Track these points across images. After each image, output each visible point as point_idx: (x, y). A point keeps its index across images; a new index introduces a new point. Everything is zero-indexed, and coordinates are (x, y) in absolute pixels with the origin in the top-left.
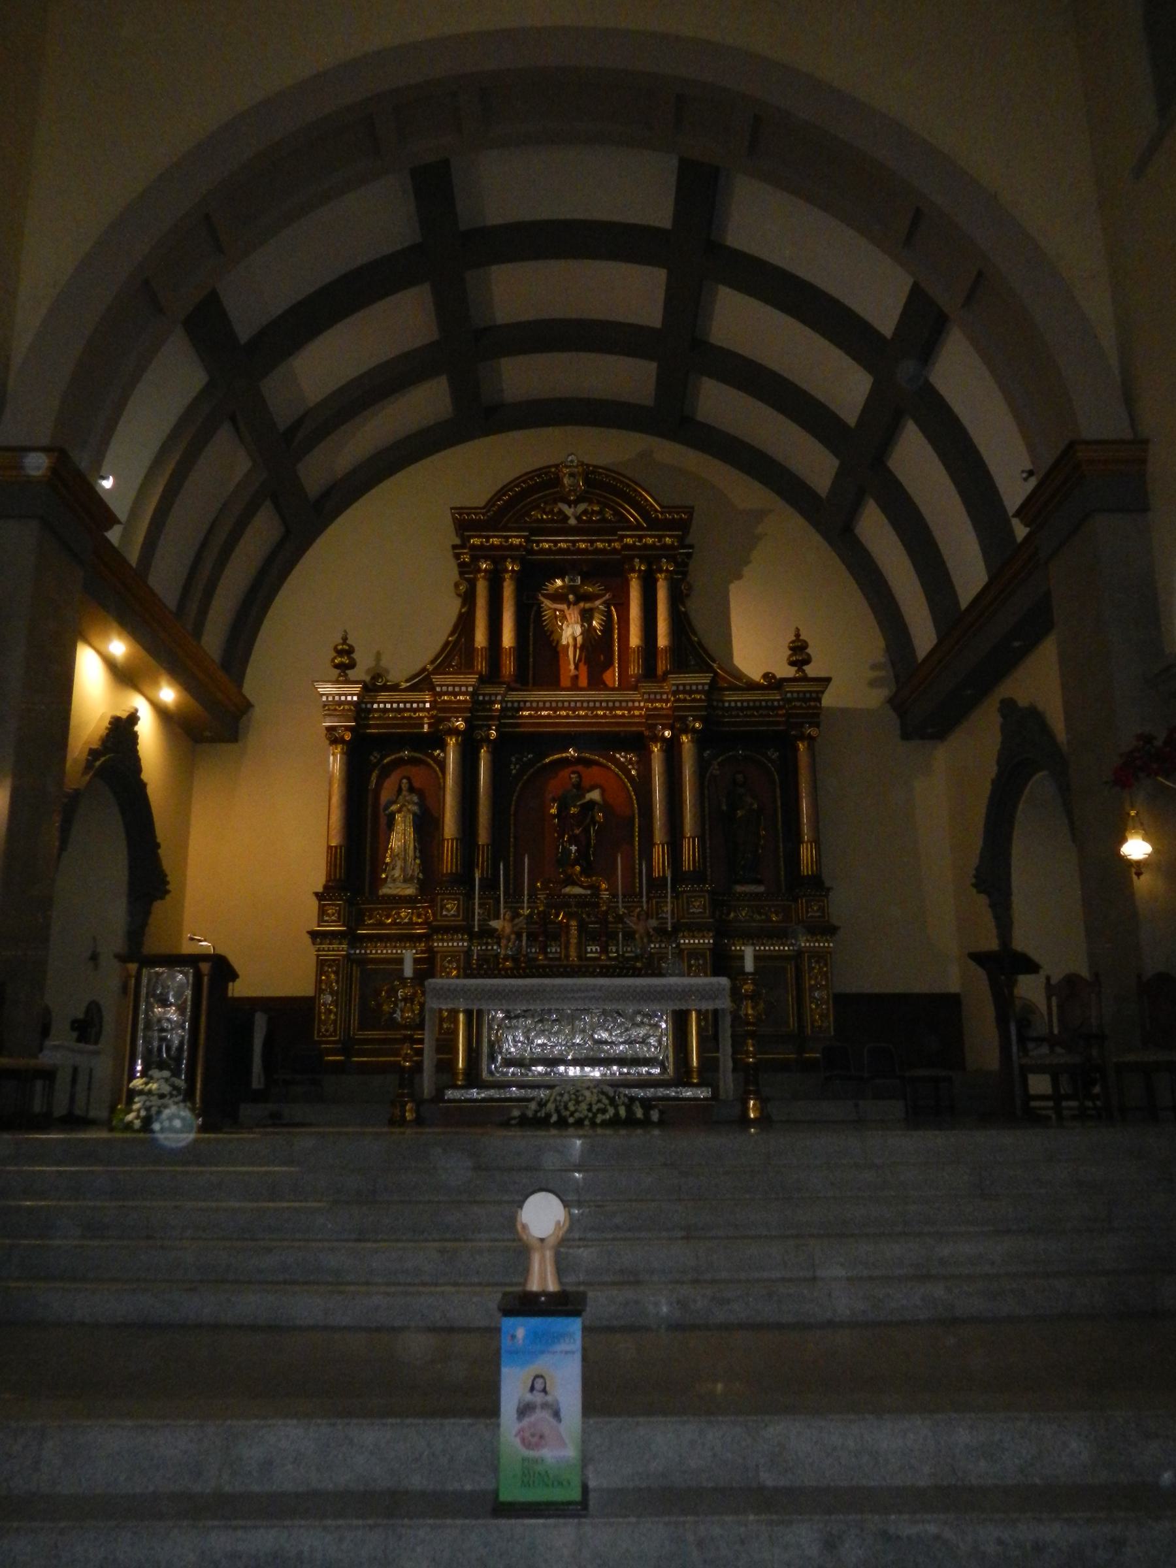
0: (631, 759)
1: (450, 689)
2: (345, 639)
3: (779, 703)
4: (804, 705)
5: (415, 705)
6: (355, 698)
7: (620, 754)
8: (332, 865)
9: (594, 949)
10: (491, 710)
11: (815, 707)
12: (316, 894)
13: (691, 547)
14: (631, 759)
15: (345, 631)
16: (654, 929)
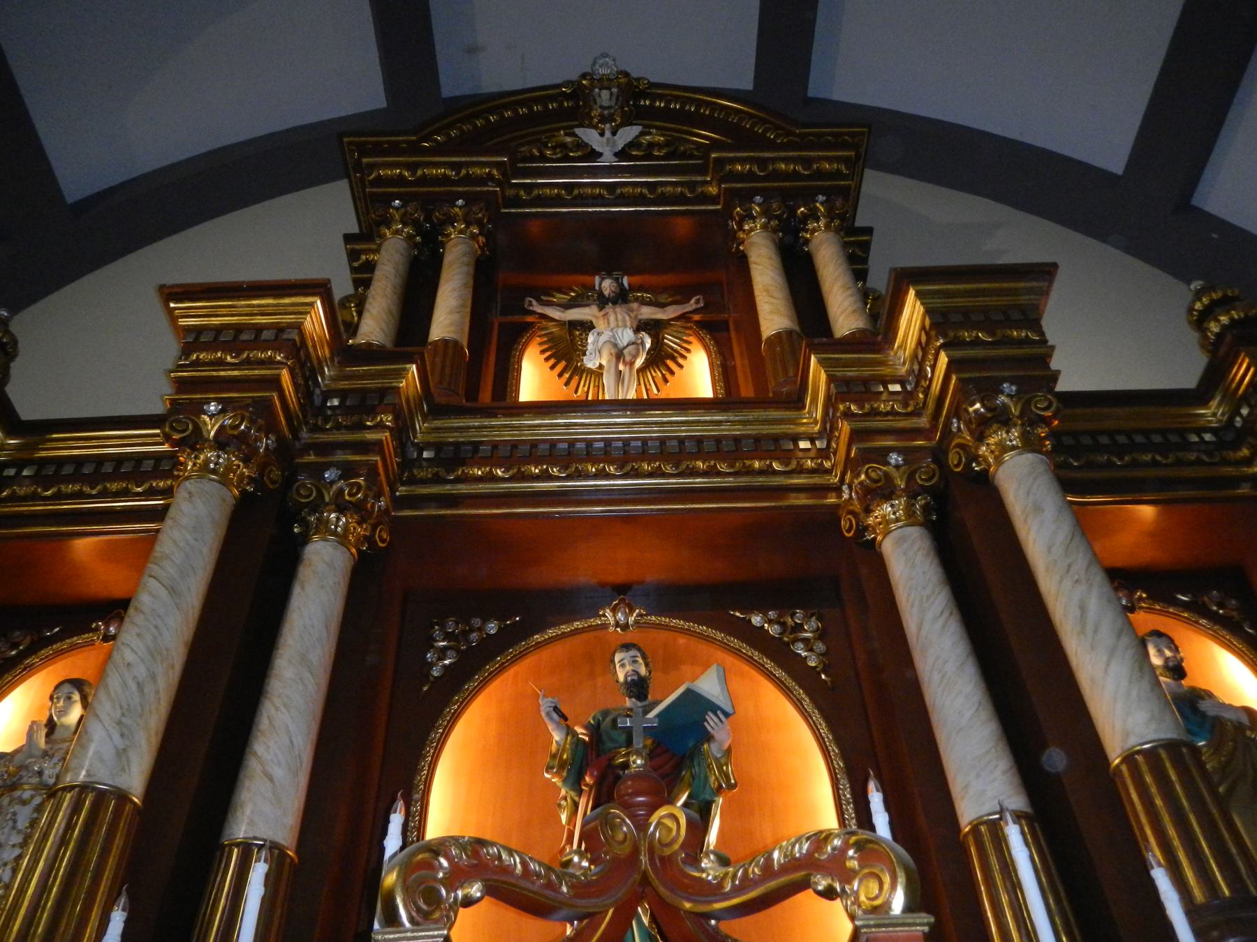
13: (869, 231)
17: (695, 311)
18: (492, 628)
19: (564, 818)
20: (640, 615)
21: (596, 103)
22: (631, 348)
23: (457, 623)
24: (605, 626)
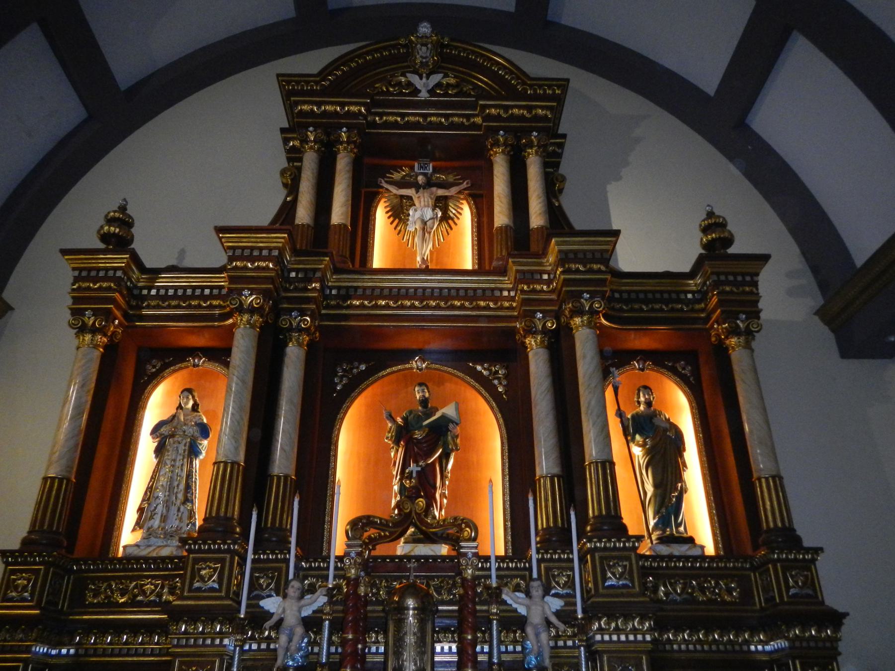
0: (497, 372)
1: (247, 253)
2: (123, 209)
3: (693, 295)
4: (735, 290)
6: (119, 273)
7: (482, 365)
8: (42, 506)
9: (446, 648)
10: (306, 290)
11: (751, 293)
13: (564, 136)
14: (497, 372)
16: (558, 614)
17: (465, 189)
18: (363, 367)
19: (392, 454)
20: (428, 364)
21: (418, 53)
22: (431, 221)
23: (347, 364)
24: (412, 368)
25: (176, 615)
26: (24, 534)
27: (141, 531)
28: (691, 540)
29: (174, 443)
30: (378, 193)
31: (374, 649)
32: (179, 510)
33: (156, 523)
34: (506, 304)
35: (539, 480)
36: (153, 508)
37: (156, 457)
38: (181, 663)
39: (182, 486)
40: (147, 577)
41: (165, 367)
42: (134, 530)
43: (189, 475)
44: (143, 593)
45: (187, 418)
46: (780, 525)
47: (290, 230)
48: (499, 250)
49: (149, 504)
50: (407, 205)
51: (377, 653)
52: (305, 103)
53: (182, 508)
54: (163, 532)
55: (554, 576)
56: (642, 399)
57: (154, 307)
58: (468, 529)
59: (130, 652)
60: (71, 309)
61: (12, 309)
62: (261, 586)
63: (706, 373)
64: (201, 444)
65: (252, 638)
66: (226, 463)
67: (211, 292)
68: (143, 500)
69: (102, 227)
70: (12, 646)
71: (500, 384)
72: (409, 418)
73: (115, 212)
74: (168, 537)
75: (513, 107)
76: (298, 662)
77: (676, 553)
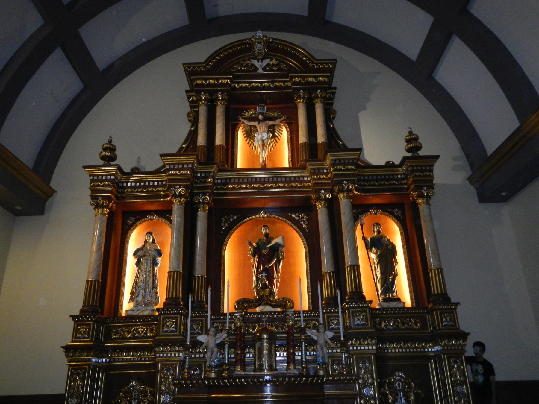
1: (176, 166)
2: (110, 142)
3: (401, 176)
4: (421, 174)
5: (156, 183)
6: (113, 177)
7: (295, 214)
8: (88, 294)
9: (282, 354)
10: (206, 182)
11: (430, 175)
12: (73, 317)
13: (335, 88)
14: (302, 218)
15: (111, 137)
17: (283, 120)
18: (235, 217)
19: (252, 261)
21: (256, 48)
22: (266, 140)
24: (260, 217)
25: (158, 344)
26: (81, 307)
27: (133, 303)
28: (399, 300)
29: (145, 260)
30: (238, 124)
31: (248, 355)
32: (150, 292)
33: (140, 299)
34: (306, 184)
35: (324, 274)
36: (138, 292)
37: (137, 266)
38: (162, 365)
39: (151, 281)
40: (139, 325)
41: (136, 221)
42: (129, 302)
43: (154, 275)
44: (138, 333)
45: (150, 247)
46: (440, 292)
47: (197, 154)
48: (302, 156)
49: (136, 290)
50: (253, 130)
51: (249, 357)
52: (198, 79)
53: (152, 291)
54: (144, 303)
55: (331, 320)
56: (375, 230)
57: (130, 192)
58: (289, 303)
59: (135, 360)
60: (90, 196)
61: (55, 192)
62: (194, 328)
63: (408, 213)
64: (158, 260)
65: (192, 353)
66: (174, 272)
67: (158, 183)
68: (133, 288)
69: (101, 152)
70: (82, 359)
71: (304, 224)
72: (259, 243)
73: (107, 144)
74: (146, 305)
75: (307, 77)
76: (216, 363)
77: (391, 306)
